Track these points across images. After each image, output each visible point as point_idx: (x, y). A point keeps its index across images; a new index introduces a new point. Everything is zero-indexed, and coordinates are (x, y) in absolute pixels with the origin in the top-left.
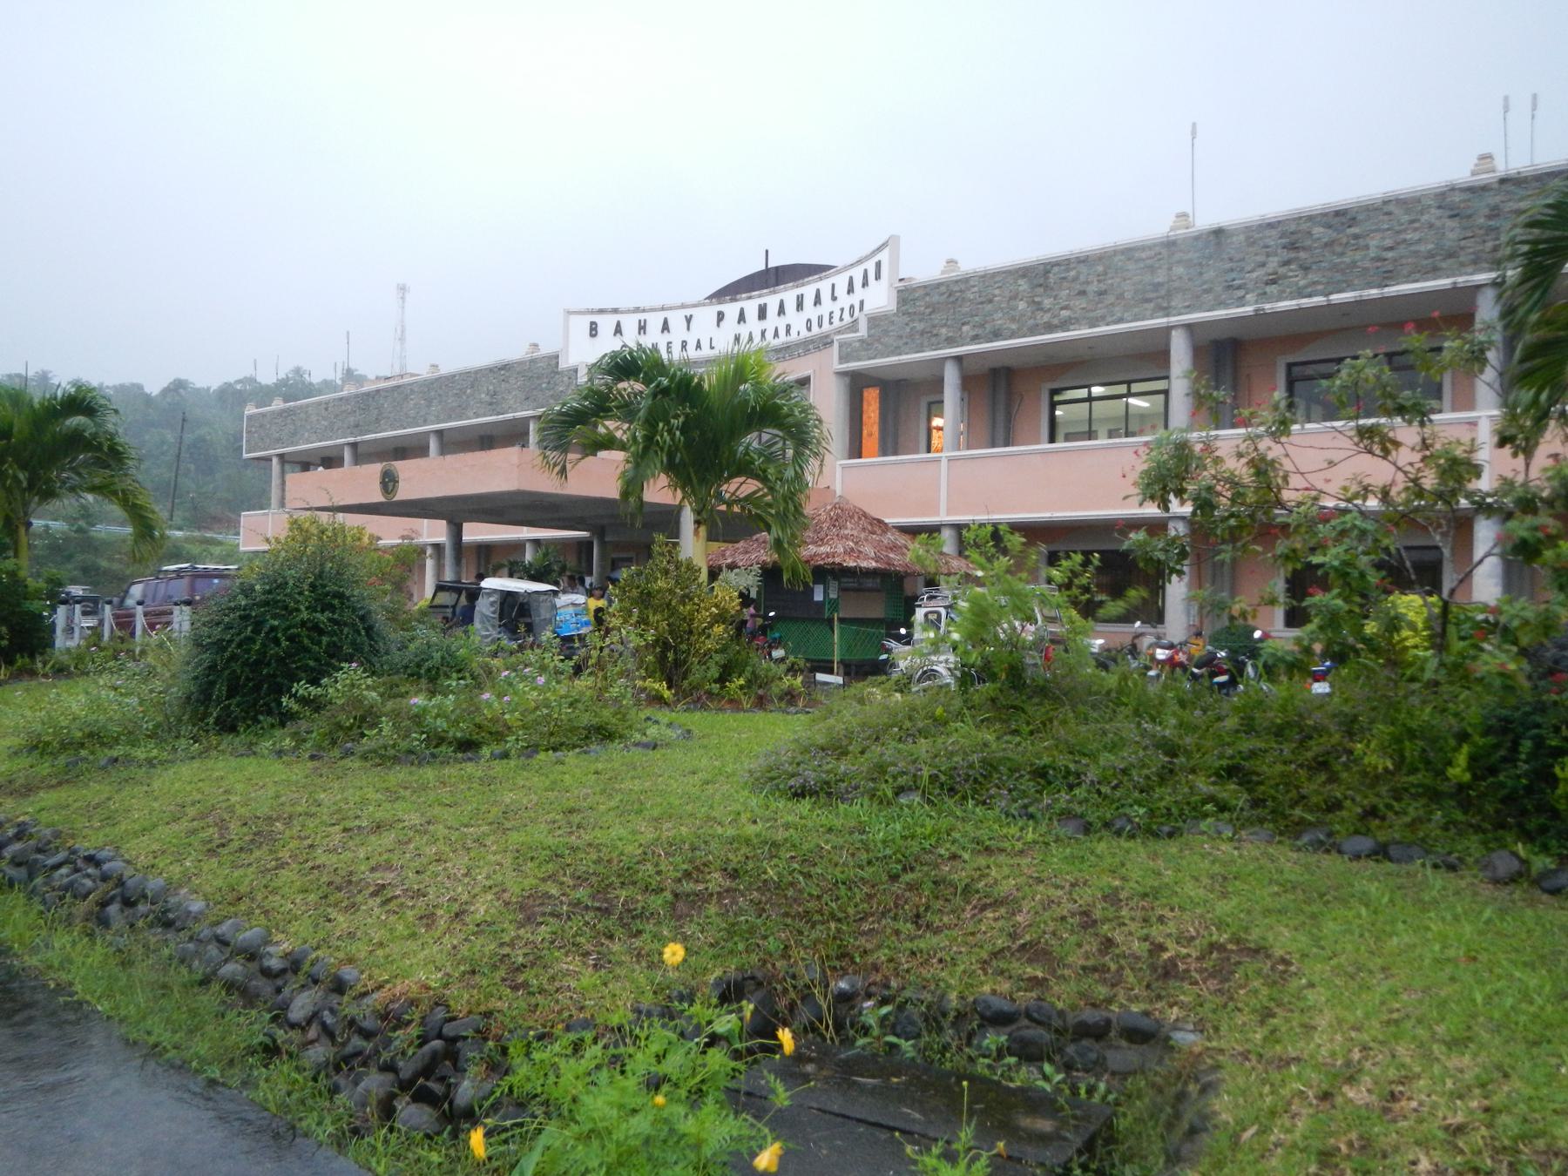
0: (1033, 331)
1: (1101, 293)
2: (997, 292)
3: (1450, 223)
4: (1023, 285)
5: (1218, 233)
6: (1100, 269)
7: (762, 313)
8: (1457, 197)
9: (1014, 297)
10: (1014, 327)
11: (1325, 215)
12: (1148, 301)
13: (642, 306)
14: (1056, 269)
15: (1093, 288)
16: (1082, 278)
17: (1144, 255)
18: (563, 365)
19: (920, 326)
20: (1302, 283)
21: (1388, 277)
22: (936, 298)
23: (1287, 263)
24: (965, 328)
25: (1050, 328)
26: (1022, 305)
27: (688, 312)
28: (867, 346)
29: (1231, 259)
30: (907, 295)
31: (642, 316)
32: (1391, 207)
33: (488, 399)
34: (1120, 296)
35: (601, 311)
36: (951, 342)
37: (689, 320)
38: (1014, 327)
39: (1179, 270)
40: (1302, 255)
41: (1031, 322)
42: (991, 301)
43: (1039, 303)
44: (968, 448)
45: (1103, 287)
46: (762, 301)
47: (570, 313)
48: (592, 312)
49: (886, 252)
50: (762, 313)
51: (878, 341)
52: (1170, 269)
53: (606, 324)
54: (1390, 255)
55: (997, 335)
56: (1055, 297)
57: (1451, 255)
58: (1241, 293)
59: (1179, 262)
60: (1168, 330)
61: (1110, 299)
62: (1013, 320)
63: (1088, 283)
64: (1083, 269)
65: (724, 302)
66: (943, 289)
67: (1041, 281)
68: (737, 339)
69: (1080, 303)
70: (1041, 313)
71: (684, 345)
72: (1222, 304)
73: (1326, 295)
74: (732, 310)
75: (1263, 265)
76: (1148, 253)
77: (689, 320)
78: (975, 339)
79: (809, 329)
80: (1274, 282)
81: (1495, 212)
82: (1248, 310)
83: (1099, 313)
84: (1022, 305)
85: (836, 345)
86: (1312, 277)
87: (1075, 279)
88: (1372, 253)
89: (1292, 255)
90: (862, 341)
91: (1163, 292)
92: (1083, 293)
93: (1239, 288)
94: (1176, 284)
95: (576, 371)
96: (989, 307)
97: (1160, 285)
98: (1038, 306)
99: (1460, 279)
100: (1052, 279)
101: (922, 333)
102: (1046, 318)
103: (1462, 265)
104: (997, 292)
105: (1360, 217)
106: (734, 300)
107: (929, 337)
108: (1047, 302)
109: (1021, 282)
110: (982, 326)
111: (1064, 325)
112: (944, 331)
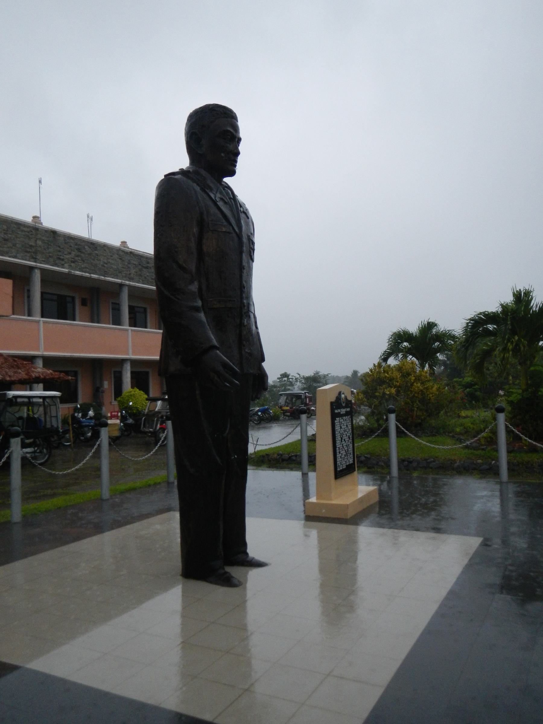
3: (120, 261)
5: (54, 233)
11: (88, 242)
12: (26, 252)
17: (25, 229)
20: (82, 266)
21: (105, 274)
23: (78, 256)
29: (59, 247)
34: (15, 245)
39: (39, 243)
40: (82, 255)
44: (113, 324)
45: (6, 237)
52: (36, 241)
54: (106, 265)
57: (120, 272)
58: (63, 262)
59: (40, 239)
60: (32, 268)
61: (10, 244)
72: (55, 265)
73: (90, 274)
75: (70, 254)
76: (29, 230)
80: (73, 262)
82: (66, 270)
86: (85, 265)
88: (102, 263)
89: (79, 253)
91: (33, 250)
93: (63, 260)
94: (39, 249)
97: (31, 246)
99: (123, 281)
103: (123, 277)
105: (98, 248)
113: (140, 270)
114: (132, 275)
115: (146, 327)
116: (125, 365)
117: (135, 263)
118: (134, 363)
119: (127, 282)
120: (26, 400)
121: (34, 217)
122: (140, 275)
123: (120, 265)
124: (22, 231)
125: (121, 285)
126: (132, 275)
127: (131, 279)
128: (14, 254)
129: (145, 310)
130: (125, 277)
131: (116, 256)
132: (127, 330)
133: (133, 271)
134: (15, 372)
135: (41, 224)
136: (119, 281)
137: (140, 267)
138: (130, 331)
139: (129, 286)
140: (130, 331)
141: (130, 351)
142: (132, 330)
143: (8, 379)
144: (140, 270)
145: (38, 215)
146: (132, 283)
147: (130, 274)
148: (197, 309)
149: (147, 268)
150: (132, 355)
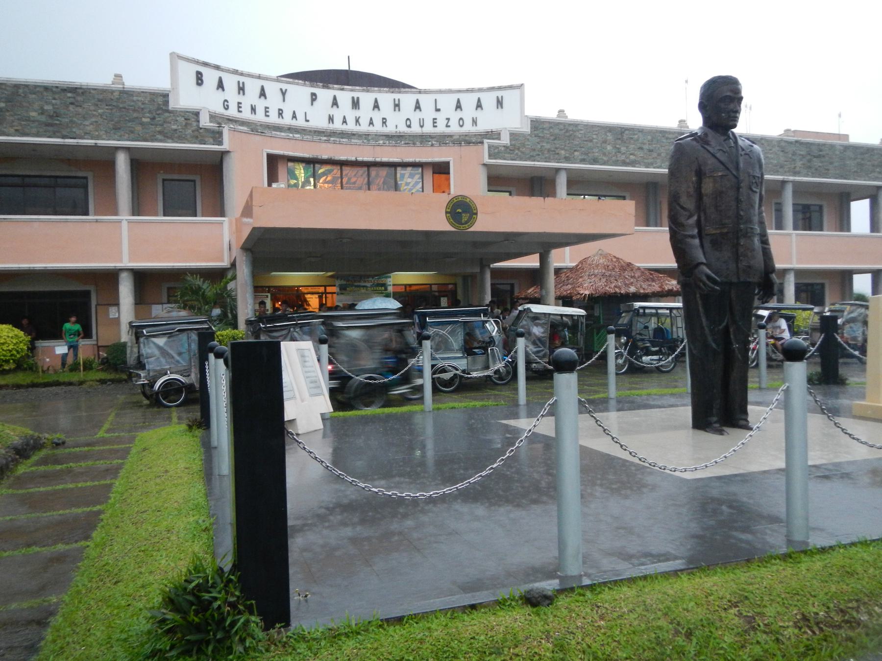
0: (616, 163)
1: (650, 151)
2: (595, 137)
3: (781, 154)
4: (610, 137)
6: (649, 138)
7: (356, 104)
8: (783, 144)
9: (605, 142)
10: (605, 159)
13: (240, 69)
14: (627, 132)
15: (646, 147)
16: (640, 140)
17: (670, 136)
18: (172, 105)
19: (548, 146)
22: (557, 131)
24: (576, 153)
25: (625, 163)
26: (609, 148)
27: (284, 86)
28: (510, 151)
30: (537, 124)
31: (242, 79)
32: (763, 142)
33: (43, 118)
34: (659, 155)
35: (206, 64)
36: (567, 159)
37: (284, 93)
38: (605, 159)
41: (614, 158)
42: (591, 141)
43: (619, 149)
45: (651, 148)
46: (355, 95)
47: (175, 57)
48: (197, 62)
49: (517, 92)
50: (356, 104)
51: (518, 149)
53: (211, 78)
55: (595, 161)
56: (627, 147)
57: (782, 167)
61: (655, 155)
62: (604, 154)
63: (644, 144)
64: (640, 134)
65: (317, 87)
66: (562, 127)
67: (620, 136)
68: (331, 119)
69: (640, 154)
70: (619, 155)
71: (280, 113)
74: (325, 95)
77: (284, 93)
78: (583, 161)
79: (409, 126)
81: (794, 154)
83: (650, 161)
84: (609, 148)
85: (486, 146)
87: (638, 140)
90: (506, 147)
92: (641, 148)
95: (197, 114)
96: (590, 144)
98: (619, 151)
100: (625, 137)
101: (549, 150)
102: (623, 157)
104: (595, 137)
106: (325, 87)
107: (553, 154)
108: (623, 149)
109: (609, 134)
110: (587, 154)
111: (633, 164)
112: (563, 152)
113: (810, 161)
114: (797, 169)
115: (821, 230)
116: (787, 276)
117: (802, 153)
118: (799, 273)
119: (791, 178)
120: (654, 311)
121: (680, 121)
122: (810, 167)
123: (782, 159)
124: (667, 138)
125: (784, 183)
126: (797, 169)
127: (795, 173)
128: (659, 164)
129: (821, 207)
130: (789, 171)
131: (776, 149)
132: (790, 235)
133: (799, 164)
134: (650, 285)
135: (688, 127)
136: (780, 178)
137: (809, 157)
138: (794, 236)
139: (793, 182)
140: (794, 236)
141: (794, 260)
142: (797, 235)
143: (642, 291)
144: (810, 161)
145: (684, 118)
146: (798, 178)
147: (795, 168)
148: (693, 237)
149: (818, 157)
150: (798, 263)
